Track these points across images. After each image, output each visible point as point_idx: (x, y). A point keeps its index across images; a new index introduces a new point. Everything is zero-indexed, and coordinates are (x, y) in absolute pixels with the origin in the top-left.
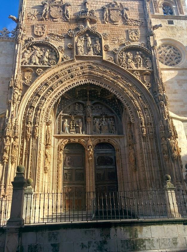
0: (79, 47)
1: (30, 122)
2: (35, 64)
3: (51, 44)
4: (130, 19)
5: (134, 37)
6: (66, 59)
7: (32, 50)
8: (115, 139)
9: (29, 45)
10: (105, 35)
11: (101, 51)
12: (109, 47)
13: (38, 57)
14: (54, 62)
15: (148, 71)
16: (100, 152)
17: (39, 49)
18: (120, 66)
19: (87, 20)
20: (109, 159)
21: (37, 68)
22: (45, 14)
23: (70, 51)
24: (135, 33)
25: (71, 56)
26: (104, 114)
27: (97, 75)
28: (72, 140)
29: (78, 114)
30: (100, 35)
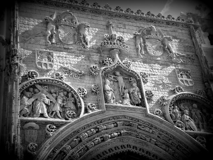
0: (109, 91)
2: (42, 115)
3: (66, 85)
4: (175, 54)
5: (186, 81)
6: (91, 109)
7: (35, 93)
9: (31, 83)
10: (144, 75)
11: (142, 99)
12: (153, 94)
13: (46, 104)
14: (74, 115)
17: (45, 91)
18: (175, 126)
19: (117, 51)
21: (47, 123)
22: (52, 36)
23: (94, 96)
24: (186, 75)
25: (97, 104)
27: (141, 138)
30: (138, 75)
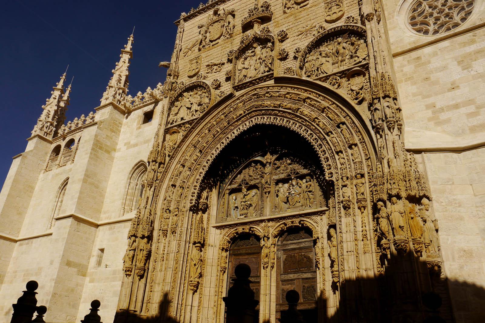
1: (168, 209)
8: (314, 217)
15: (358, 68)
16: (289, 248)
20: (305, 259)
26: (294, 173)
27: (267, 107)
28: (240, 229)
29: (252, 183)
